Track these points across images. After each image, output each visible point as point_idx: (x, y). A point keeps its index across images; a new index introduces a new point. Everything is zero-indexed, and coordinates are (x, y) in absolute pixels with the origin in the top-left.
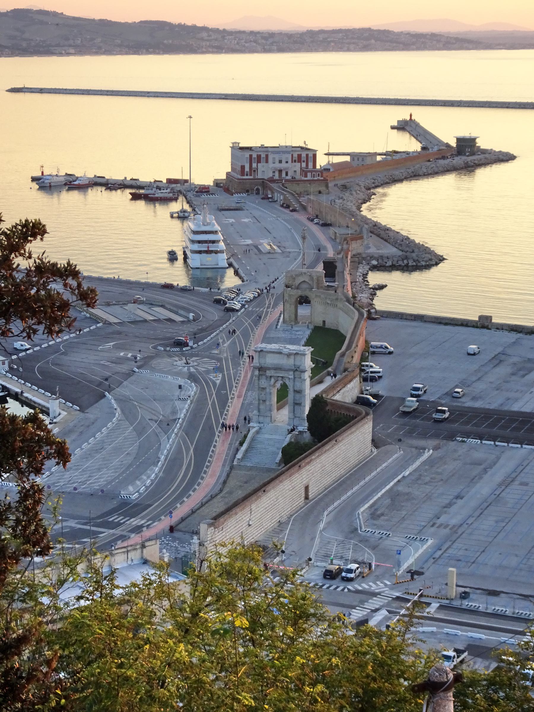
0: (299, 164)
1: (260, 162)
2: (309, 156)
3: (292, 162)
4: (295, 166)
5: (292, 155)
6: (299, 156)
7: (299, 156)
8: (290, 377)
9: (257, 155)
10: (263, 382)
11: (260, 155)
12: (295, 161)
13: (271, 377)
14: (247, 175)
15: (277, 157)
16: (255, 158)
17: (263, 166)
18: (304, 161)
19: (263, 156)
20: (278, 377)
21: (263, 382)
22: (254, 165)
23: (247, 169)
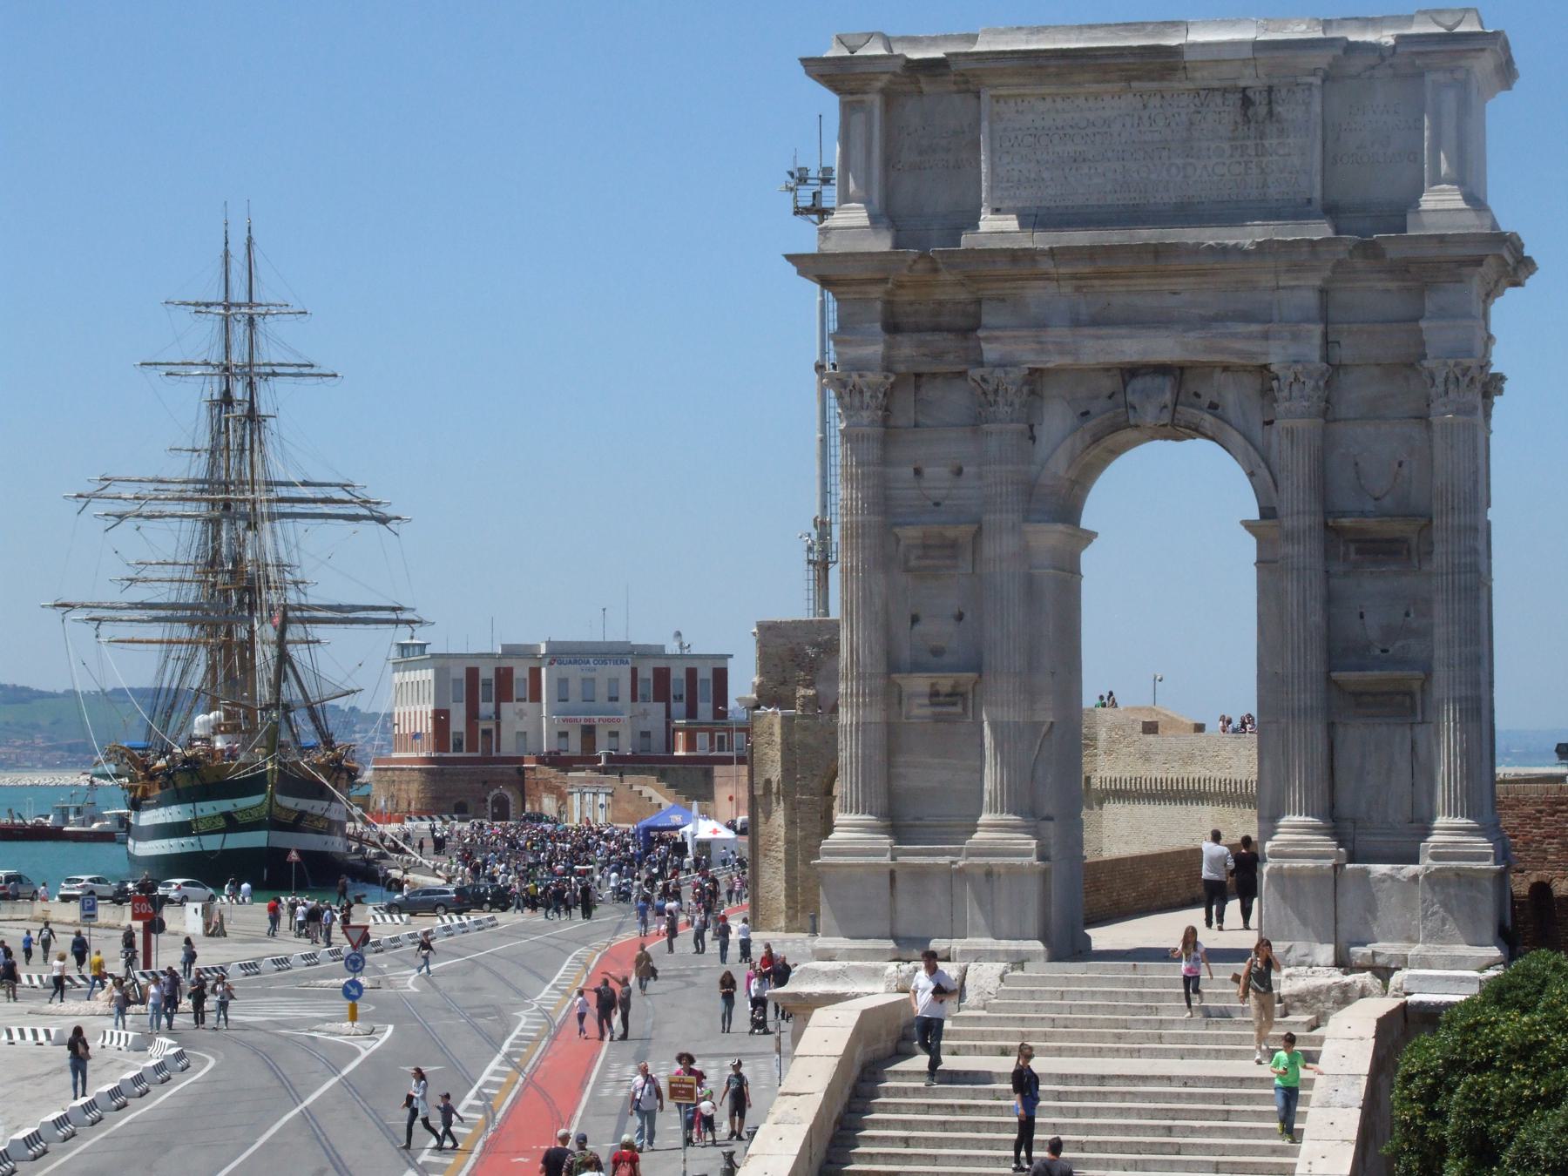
0: (662, 706)
1: (509, 699)
2: (700, 675)
3: (634, 698)
4: (645, 714)
5: (634, 671)
6: (662, 676)
7: (662, 676)
8: (1276, 355)
9: (498, 670)
10: (937, 474)
11: (509, 671)
12: (645, 699)
13: (1036, 374)
14: (458, 747)
15: (573, 672)
16: (487, 683)
17: (521, 714)
18: (679, 698)
19: (521, 672)
20: (1130, 372)
21: (937, 474)
22: (486, 708)
23: (458, 724)
